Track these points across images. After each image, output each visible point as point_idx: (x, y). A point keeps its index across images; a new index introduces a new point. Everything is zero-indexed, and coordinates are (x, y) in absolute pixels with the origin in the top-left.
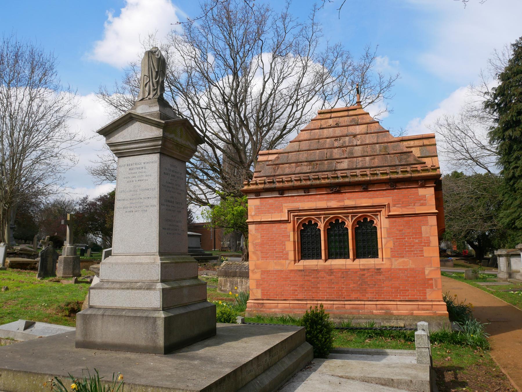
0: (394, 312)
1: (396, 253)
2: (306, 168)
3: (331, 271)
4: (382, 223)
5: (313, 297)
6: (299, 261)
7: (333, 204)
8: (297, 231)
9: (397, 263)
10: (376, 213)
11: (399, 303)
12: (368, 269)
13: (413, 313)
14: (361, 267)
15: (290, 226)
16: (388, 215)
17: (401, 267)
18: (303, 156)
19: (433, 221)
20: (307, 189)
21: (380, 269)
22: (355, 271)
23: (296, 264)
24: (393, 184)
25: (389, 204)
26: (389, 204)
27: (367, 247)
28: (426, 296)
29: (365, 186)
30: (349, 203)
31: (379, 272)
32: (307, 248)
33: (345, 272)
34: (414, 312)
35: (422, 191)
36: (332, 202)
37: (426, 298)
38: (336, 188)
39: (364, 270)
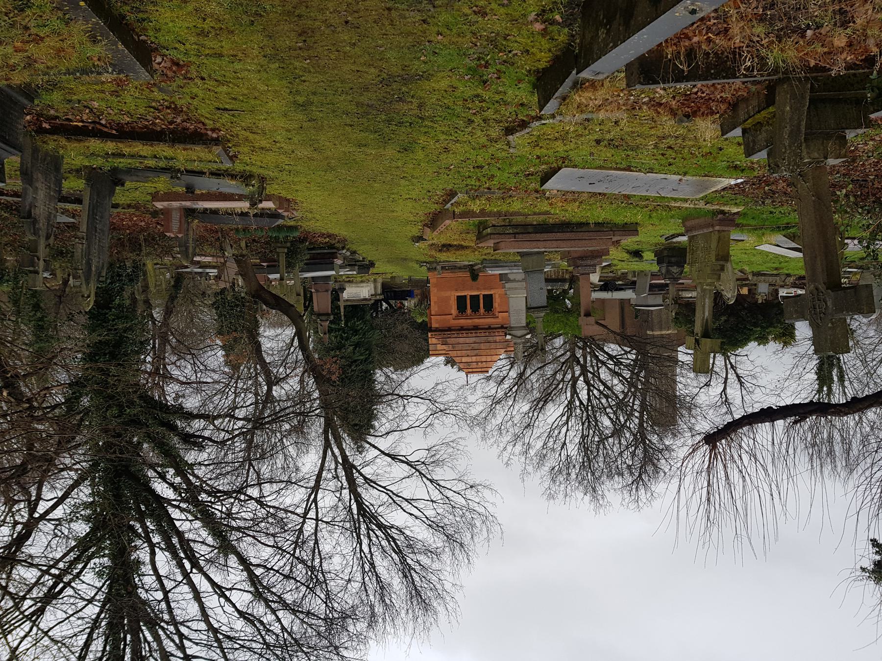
1: (448, 298)
2: (491, 339)
3: (478, 289)
4: (454, 311)
7: (477, 321)
9: (448, 294)
10: (457, 316)
15: (498, 310)
18: (493, 345)
19: (433, 313)
20: (490, 328)
22: (467, 289)
24: (449, 329)
27: (461, 300)
29: (462, 329)
30: (470, 321)
32: (489, 299)
33: (471, 289)
35: (437, 326)
36: (477, 321)
38: (476, 328)
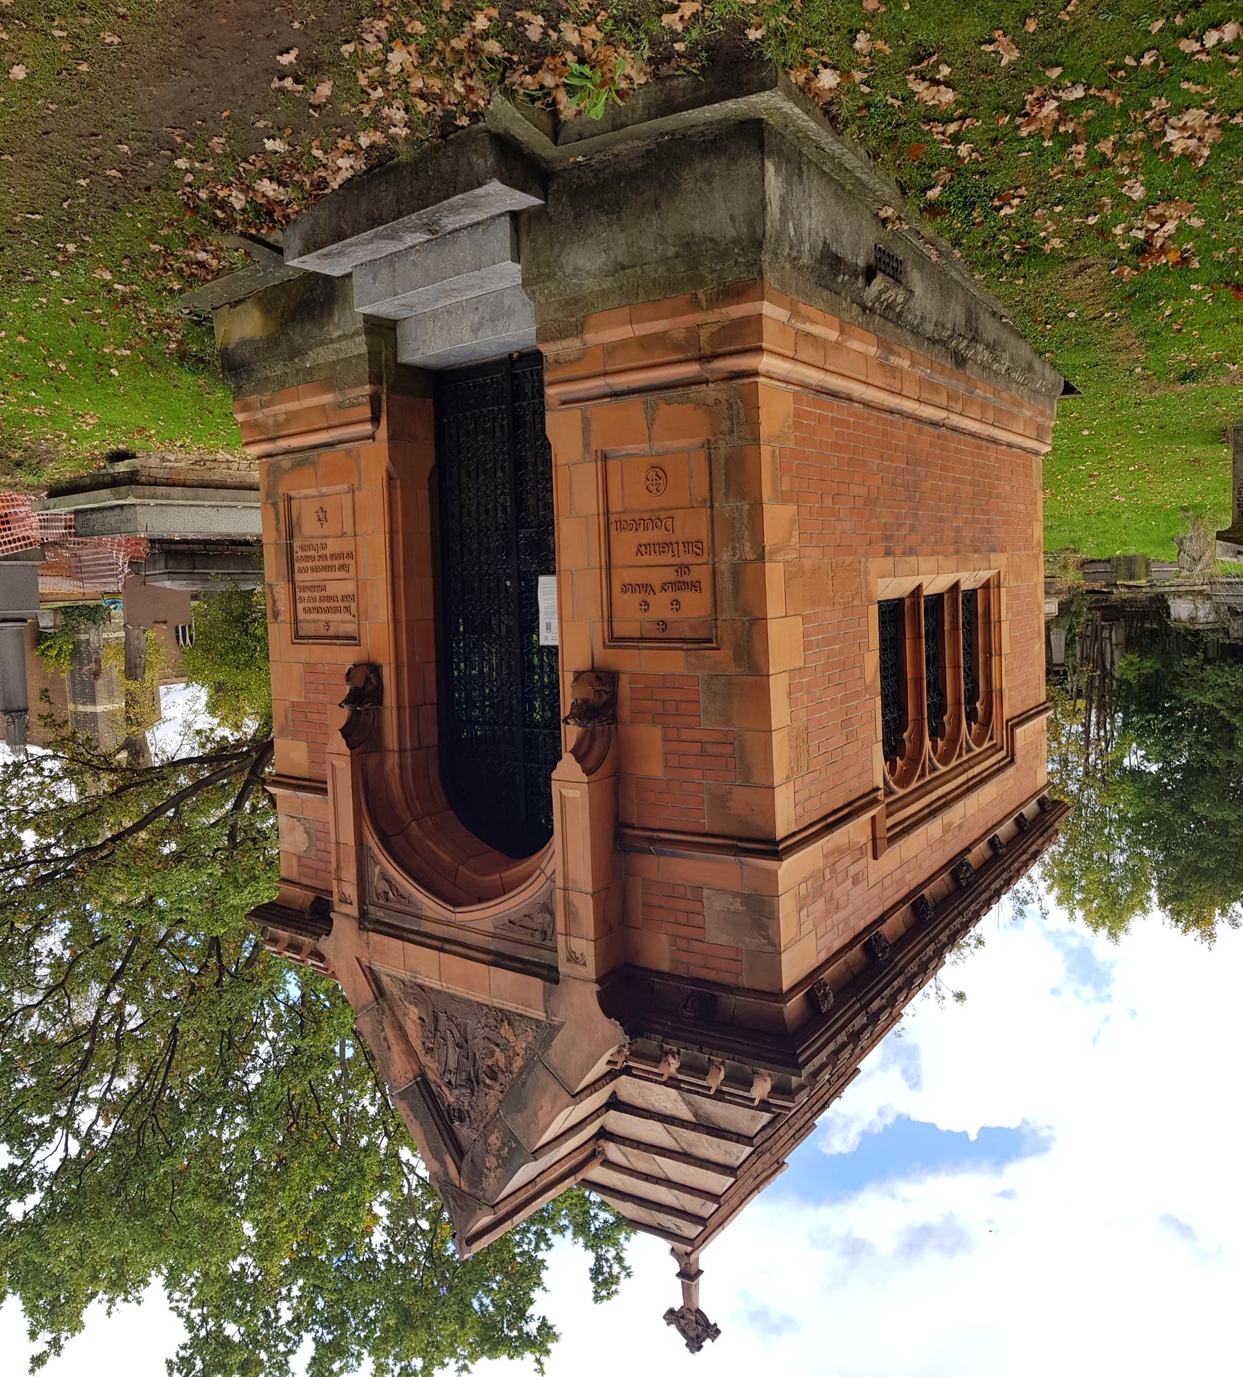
0: (872, 350)
5: (979, 447)
6: (986, 586)
8: (989, 693)
11: (858, 390)
12: (904, 553)
13: (842, 332)
14: (914, 559)
16: (875, 802)
17: (848, 559)
21: (888, 553)
23: (993, 572)
25: (875, 857)
26: (875, 857)
28: (798, 414)
31: (887, 538)
34: (833, 335)
37: (797, 398)
39: (911, 552)
